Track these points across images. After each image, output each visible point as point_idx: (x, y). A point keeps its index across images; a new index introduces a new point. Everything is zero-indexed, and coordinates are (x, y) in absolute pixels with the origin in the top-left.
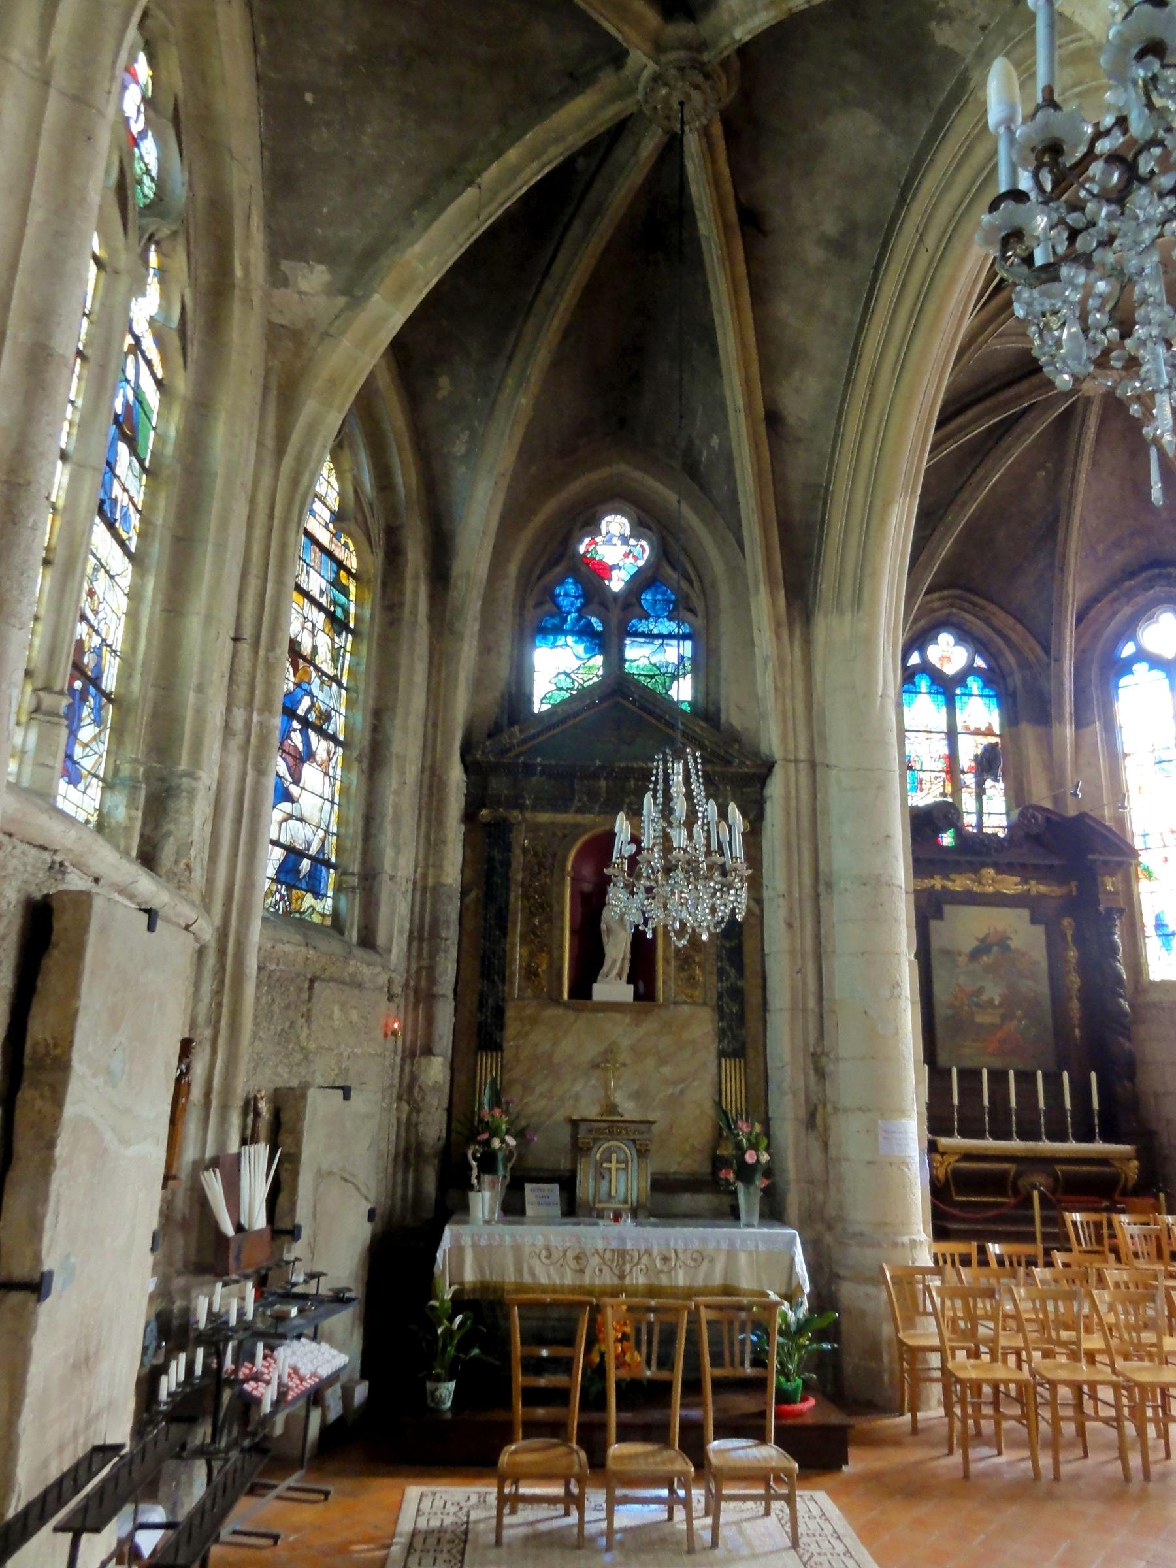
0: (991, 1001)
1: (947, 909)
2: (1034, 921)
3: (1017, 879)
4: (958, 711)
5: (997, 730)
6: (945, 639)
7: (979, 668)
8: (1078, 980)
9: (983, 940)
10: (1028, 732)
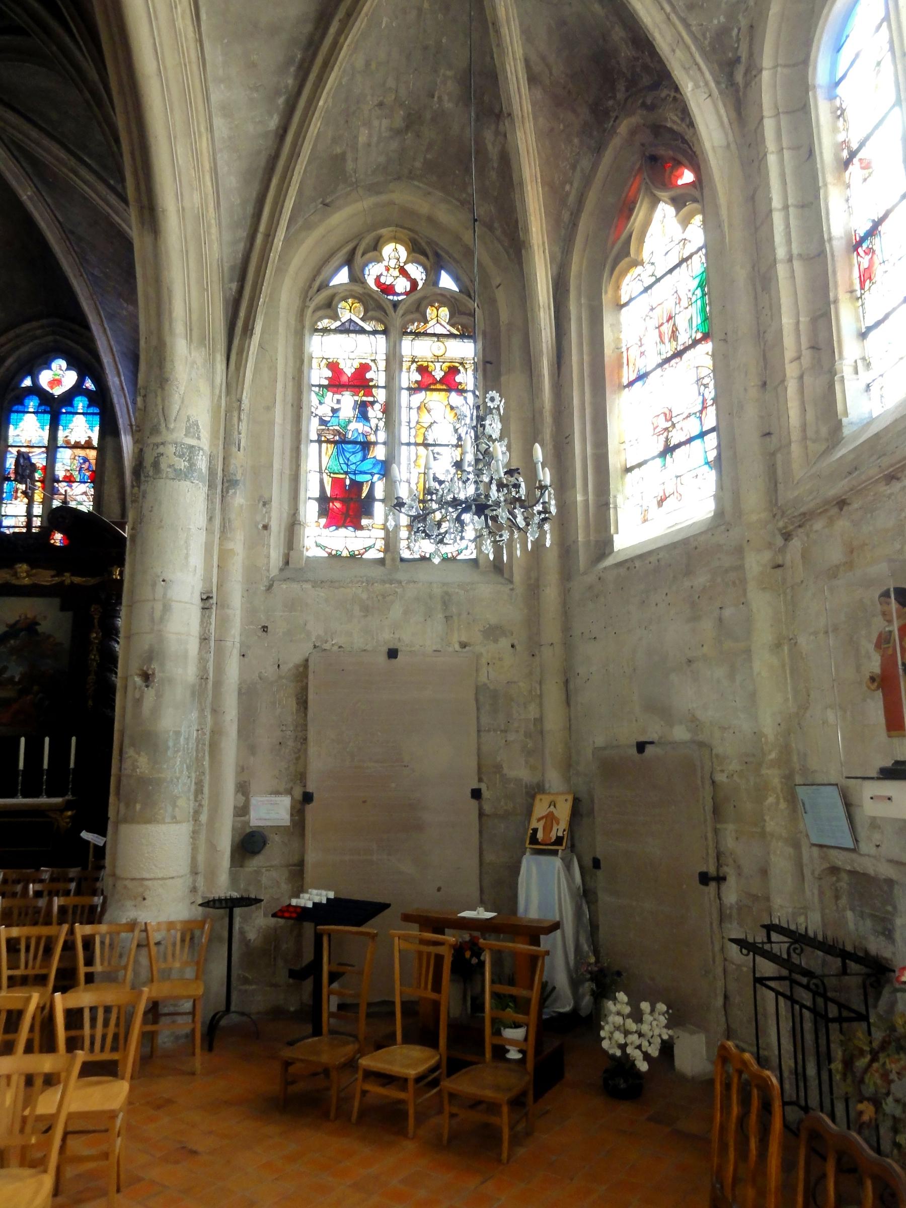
0: (13, 677)
2: (63, 608)
3: (53, 573)
4: (61, 428)
5: (95, 443)
6: (60, 364)
7: (87, 389)
8: (97, 657)
9: (12, 626)
10: (109, 440)
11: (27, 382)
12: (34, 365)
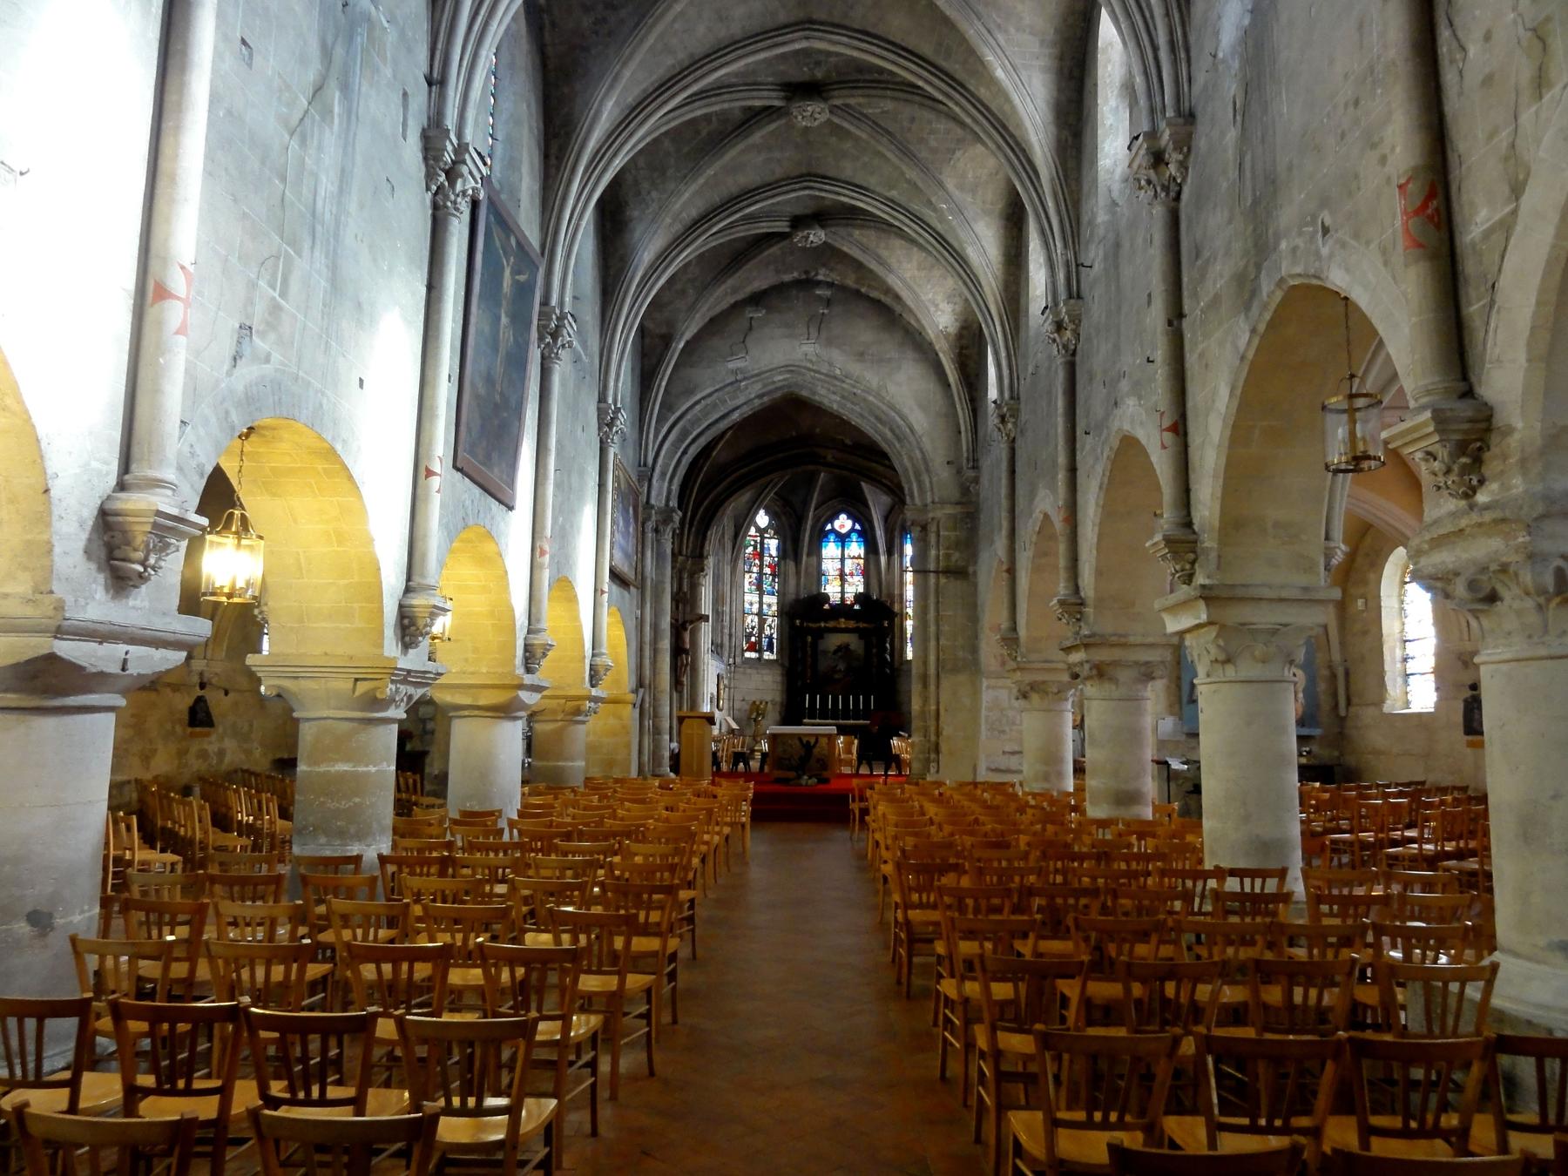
1: (826, 635)
2: (860, 638)
6: (843, 517)
10: (872, 557)
11: (829, 527)
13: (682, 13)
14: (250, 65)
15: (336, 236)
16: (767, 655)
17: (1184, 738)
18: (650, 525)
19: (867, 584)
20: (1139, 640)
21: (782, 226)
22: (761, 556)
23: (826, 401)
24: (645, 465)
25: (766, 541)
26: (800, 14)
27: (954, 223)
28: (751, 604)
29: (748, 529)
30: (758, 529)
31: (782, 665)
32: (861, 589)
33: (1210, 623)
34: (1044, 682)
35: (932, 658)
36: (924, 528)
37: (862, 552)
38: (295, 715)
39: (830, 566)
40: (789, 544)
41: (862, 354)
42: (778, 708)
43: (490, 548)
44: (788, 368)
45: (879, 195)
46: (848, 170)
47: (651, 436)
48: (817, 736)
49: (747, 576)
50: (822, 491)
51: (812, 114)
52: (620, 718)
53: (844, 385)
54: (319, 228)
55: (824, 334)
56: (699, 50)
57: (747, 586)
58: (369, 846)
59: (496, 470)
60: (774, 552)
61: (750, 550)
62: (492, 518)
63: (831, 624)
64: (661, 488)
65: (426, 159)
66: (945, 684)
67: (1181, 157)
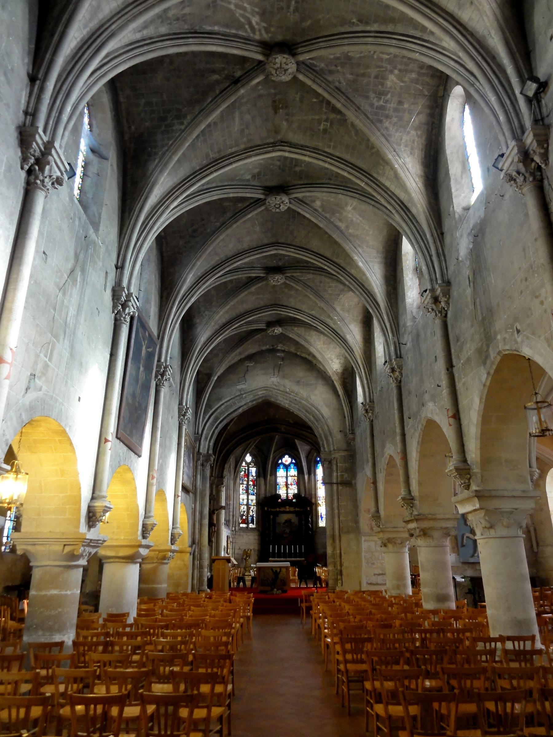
2: (296, 516)
6: (287, 457)
10: (301, 476)
11: (280, 461)
12: (282, 457)
13: (223, 240)
14: (46, 262)
15: (74, 334)
16: (251, 526)
17: (460, 565)
18: (199, 462)
19: (299, 489)
20: (442, 516)
21: (263, 326)
22: (247, 475)
23: (282, 403)
24: (198, 433)
25: (250, 469)
26: (273, 240)
27: (341, 325)
28: (243, 500)
29: (242, 463)
30: (246, 463)
31: (258, 530)
32: (296, 492)
33: (481, 509)
34: (394, 538)
35: (337, 526)
36: (330, 462)
37: (296, 473)
38: (31, 564)
39: (281, 480)
40: (261, 469)
41: (298, 382)
42: (256, 552)
43: (129, 476)
44: (266, 388)
45: (306, 313)
46: (292, 302)
47: (201, 420)
48: (281, 568)
49: (241, 486)
50: (276, 444)
51: (278, 280)
52: (183, 561)
53: (291, 396)
54: (67, 330)
55: (281, 373)
56: (230, 254)
57: (241, 491)
58: (64, 635)
59: (134, 438)
60: (254, 474)
61: (243, 473)
62: (132, 461)
63: (282, 509)
64: (205, 444)
65: (113, 299)
66: (344, 539)
67: (446, 299)
